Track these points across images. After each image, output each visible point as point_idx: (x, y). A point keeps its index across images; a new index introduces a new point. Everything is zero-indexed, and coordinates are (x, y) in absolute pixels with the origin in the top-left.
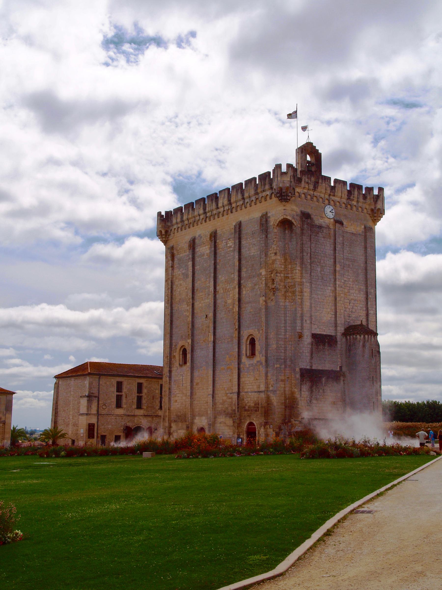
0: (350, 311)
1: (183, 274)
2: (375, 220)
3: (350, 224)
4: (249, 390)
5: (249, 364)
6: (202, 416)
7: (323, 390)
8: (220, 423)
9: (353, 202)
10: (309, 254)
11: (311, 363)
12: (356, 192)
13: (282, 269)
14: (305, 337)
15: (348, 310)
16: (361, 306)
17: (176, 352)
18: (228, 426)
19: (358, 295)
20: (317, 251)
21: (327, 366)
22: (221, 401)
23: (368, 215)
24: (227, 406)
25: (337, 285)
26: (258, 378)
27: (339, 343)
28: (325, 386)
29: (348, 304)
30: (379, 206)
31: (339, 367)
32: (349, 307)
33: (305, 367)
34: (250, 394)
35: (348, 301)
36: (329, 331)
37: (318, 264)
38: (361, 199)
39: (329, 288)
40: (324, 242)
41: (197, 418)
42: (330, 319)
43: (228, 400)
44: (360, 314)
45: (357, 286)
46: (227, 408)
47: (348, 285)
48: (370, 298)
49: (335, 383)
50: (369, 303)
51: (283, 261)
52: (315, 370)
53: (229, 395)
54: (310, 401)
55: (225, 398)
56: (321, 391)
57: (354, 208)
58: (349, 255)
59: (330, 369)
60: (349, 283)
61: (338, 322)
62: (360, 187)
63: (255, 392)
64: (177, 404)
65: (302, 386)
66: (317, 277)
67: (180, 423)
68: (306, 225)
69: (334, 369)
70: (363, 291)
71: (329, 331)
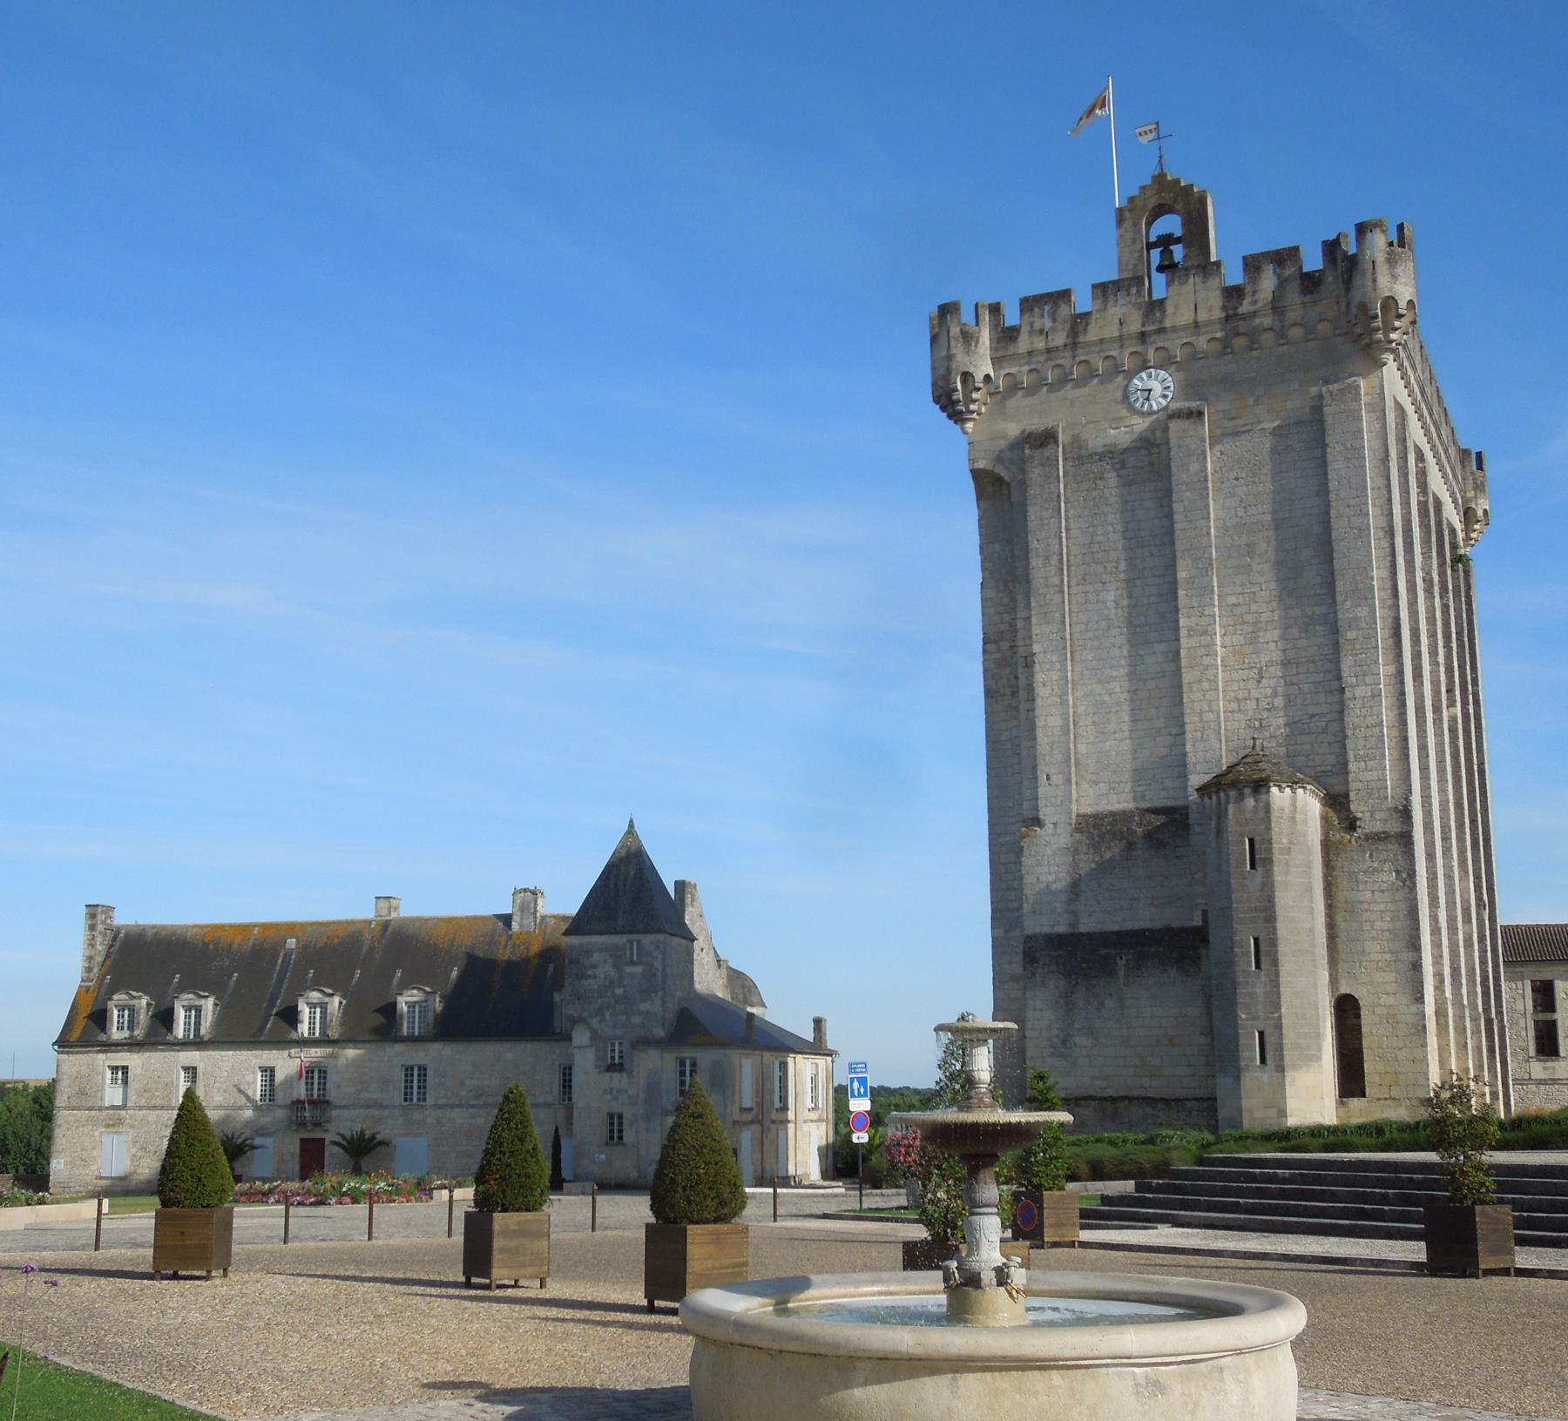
0: (1263, 704)
2: (1368, 346)
3: (1251, 401)
7: (1121, 999)
9: (1257, 321)
10: (1054, 560)
11: (1075, 913)
12: (1268, 282)
13: (1003, 627)
14: (1049, 827)
15: (1251, 705)
16: (1319, 677)
19: (1303, 643)
20: (1099, 538)
21: (1145, 917)
23: (1341, 340)
25: (1183, 633)
27: (1197, 829)
28: (1127, 985)
29: (1252, 684)
30: (1357, 297)
31: (1199, 913)
32: (1255, 694)
33: (1046, 930)
35: (1253, 674)
36: (1163, 794)
37: (1105, 578)
38: (1293, 297)
39: (1159, 648)
40: (1130, 498)
42: (1164, 751)
44: (1312, 710)
45: (1297, 612)
47: (1249, 618)
48: (1352, 642)
49: (1173, 972)
50: (1346, 665)
51: (1006, 601)
52: (1090, 936)
54: (1064, 1042)
56: (1110, 1003)
57: (1267, 339)
58: (1250, 511)
59: (1158, 925)
60: (1254, 607)
61: (1191, 759)
62: (1284, 257)
65: (1029, 994)
66: (1103, 624)
68: (1037, 471)
69: (1175, 924)
70: (1325, 624)
71: (1163, 794)
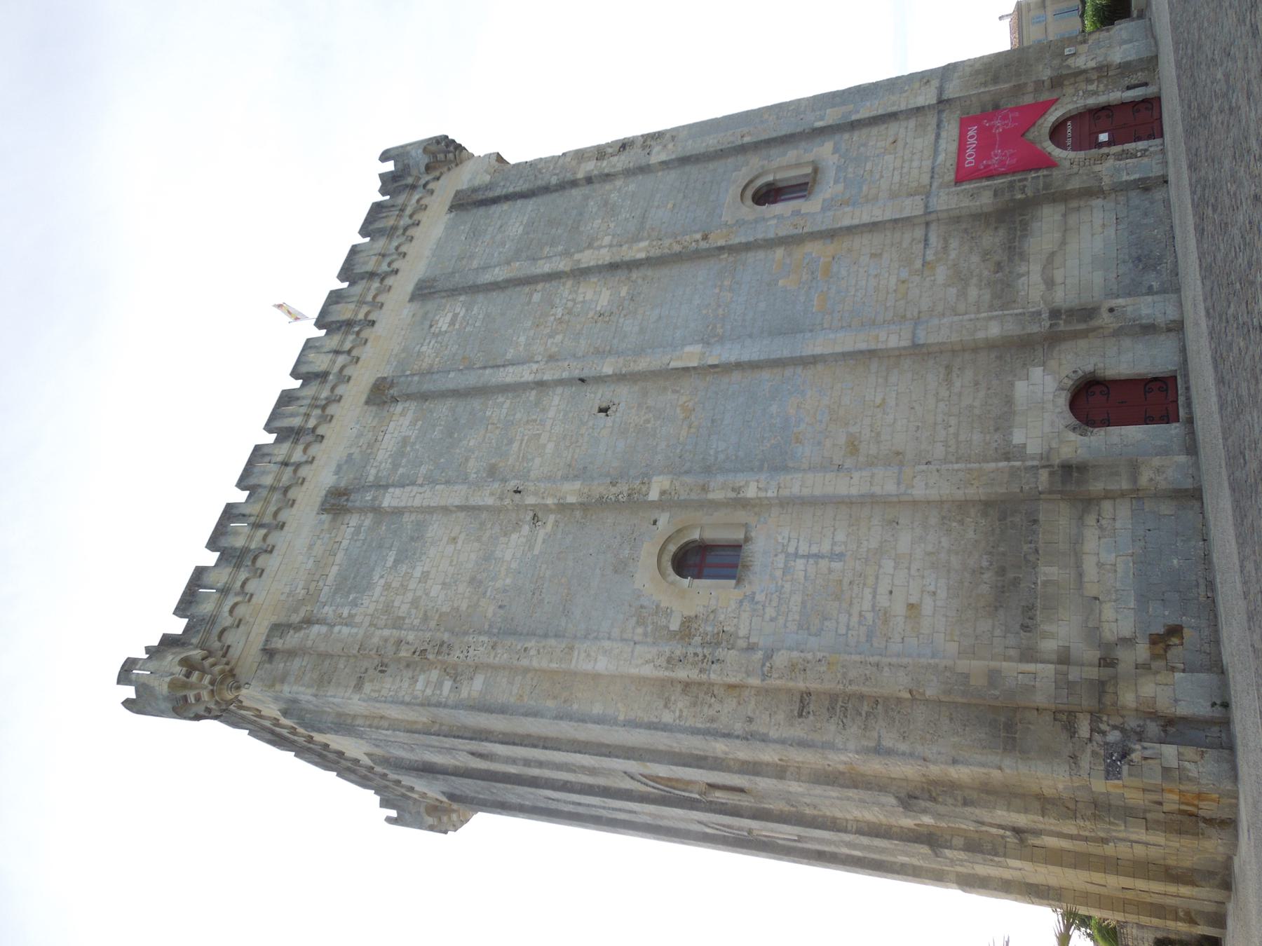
1: (396, 562)
4: (927, 164)
5: (836, 182)
6: (1009, 401)
8: (1050, 283)
17: (668, 613)
18: (1063, 243)
22: (953, 291)
24: (975, 259)
26: (891, 140)
34: (941, 158)
41: (1018, 437)
43: (953, 255)
46: (985, 255)
53: (930, 256)
55: (941, 273)
63: (938, 136)
64: (927, 607)
67: (1049, 571)
